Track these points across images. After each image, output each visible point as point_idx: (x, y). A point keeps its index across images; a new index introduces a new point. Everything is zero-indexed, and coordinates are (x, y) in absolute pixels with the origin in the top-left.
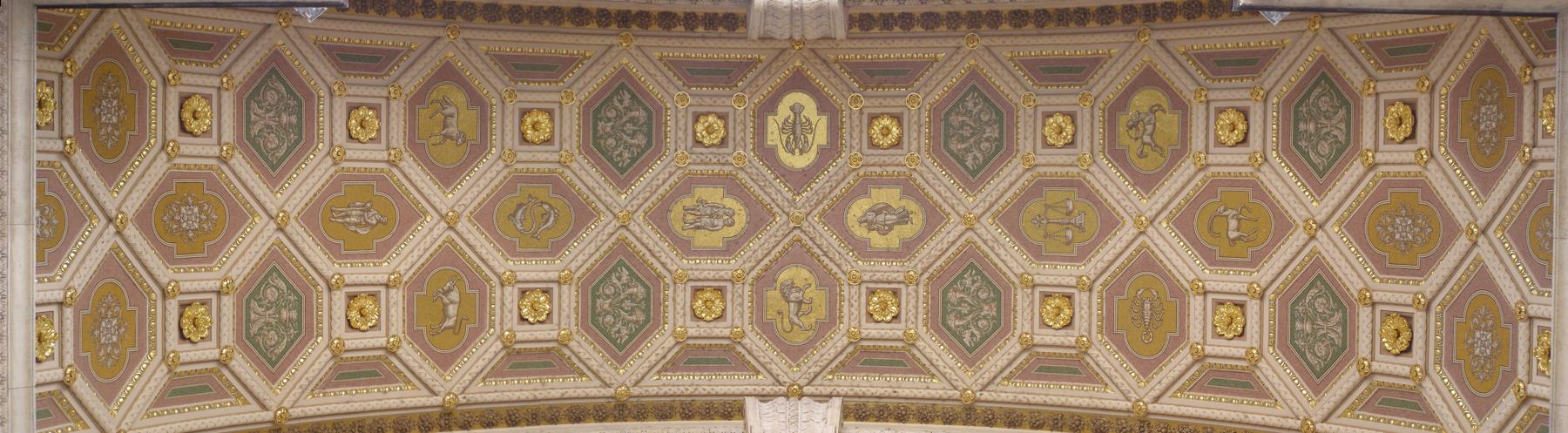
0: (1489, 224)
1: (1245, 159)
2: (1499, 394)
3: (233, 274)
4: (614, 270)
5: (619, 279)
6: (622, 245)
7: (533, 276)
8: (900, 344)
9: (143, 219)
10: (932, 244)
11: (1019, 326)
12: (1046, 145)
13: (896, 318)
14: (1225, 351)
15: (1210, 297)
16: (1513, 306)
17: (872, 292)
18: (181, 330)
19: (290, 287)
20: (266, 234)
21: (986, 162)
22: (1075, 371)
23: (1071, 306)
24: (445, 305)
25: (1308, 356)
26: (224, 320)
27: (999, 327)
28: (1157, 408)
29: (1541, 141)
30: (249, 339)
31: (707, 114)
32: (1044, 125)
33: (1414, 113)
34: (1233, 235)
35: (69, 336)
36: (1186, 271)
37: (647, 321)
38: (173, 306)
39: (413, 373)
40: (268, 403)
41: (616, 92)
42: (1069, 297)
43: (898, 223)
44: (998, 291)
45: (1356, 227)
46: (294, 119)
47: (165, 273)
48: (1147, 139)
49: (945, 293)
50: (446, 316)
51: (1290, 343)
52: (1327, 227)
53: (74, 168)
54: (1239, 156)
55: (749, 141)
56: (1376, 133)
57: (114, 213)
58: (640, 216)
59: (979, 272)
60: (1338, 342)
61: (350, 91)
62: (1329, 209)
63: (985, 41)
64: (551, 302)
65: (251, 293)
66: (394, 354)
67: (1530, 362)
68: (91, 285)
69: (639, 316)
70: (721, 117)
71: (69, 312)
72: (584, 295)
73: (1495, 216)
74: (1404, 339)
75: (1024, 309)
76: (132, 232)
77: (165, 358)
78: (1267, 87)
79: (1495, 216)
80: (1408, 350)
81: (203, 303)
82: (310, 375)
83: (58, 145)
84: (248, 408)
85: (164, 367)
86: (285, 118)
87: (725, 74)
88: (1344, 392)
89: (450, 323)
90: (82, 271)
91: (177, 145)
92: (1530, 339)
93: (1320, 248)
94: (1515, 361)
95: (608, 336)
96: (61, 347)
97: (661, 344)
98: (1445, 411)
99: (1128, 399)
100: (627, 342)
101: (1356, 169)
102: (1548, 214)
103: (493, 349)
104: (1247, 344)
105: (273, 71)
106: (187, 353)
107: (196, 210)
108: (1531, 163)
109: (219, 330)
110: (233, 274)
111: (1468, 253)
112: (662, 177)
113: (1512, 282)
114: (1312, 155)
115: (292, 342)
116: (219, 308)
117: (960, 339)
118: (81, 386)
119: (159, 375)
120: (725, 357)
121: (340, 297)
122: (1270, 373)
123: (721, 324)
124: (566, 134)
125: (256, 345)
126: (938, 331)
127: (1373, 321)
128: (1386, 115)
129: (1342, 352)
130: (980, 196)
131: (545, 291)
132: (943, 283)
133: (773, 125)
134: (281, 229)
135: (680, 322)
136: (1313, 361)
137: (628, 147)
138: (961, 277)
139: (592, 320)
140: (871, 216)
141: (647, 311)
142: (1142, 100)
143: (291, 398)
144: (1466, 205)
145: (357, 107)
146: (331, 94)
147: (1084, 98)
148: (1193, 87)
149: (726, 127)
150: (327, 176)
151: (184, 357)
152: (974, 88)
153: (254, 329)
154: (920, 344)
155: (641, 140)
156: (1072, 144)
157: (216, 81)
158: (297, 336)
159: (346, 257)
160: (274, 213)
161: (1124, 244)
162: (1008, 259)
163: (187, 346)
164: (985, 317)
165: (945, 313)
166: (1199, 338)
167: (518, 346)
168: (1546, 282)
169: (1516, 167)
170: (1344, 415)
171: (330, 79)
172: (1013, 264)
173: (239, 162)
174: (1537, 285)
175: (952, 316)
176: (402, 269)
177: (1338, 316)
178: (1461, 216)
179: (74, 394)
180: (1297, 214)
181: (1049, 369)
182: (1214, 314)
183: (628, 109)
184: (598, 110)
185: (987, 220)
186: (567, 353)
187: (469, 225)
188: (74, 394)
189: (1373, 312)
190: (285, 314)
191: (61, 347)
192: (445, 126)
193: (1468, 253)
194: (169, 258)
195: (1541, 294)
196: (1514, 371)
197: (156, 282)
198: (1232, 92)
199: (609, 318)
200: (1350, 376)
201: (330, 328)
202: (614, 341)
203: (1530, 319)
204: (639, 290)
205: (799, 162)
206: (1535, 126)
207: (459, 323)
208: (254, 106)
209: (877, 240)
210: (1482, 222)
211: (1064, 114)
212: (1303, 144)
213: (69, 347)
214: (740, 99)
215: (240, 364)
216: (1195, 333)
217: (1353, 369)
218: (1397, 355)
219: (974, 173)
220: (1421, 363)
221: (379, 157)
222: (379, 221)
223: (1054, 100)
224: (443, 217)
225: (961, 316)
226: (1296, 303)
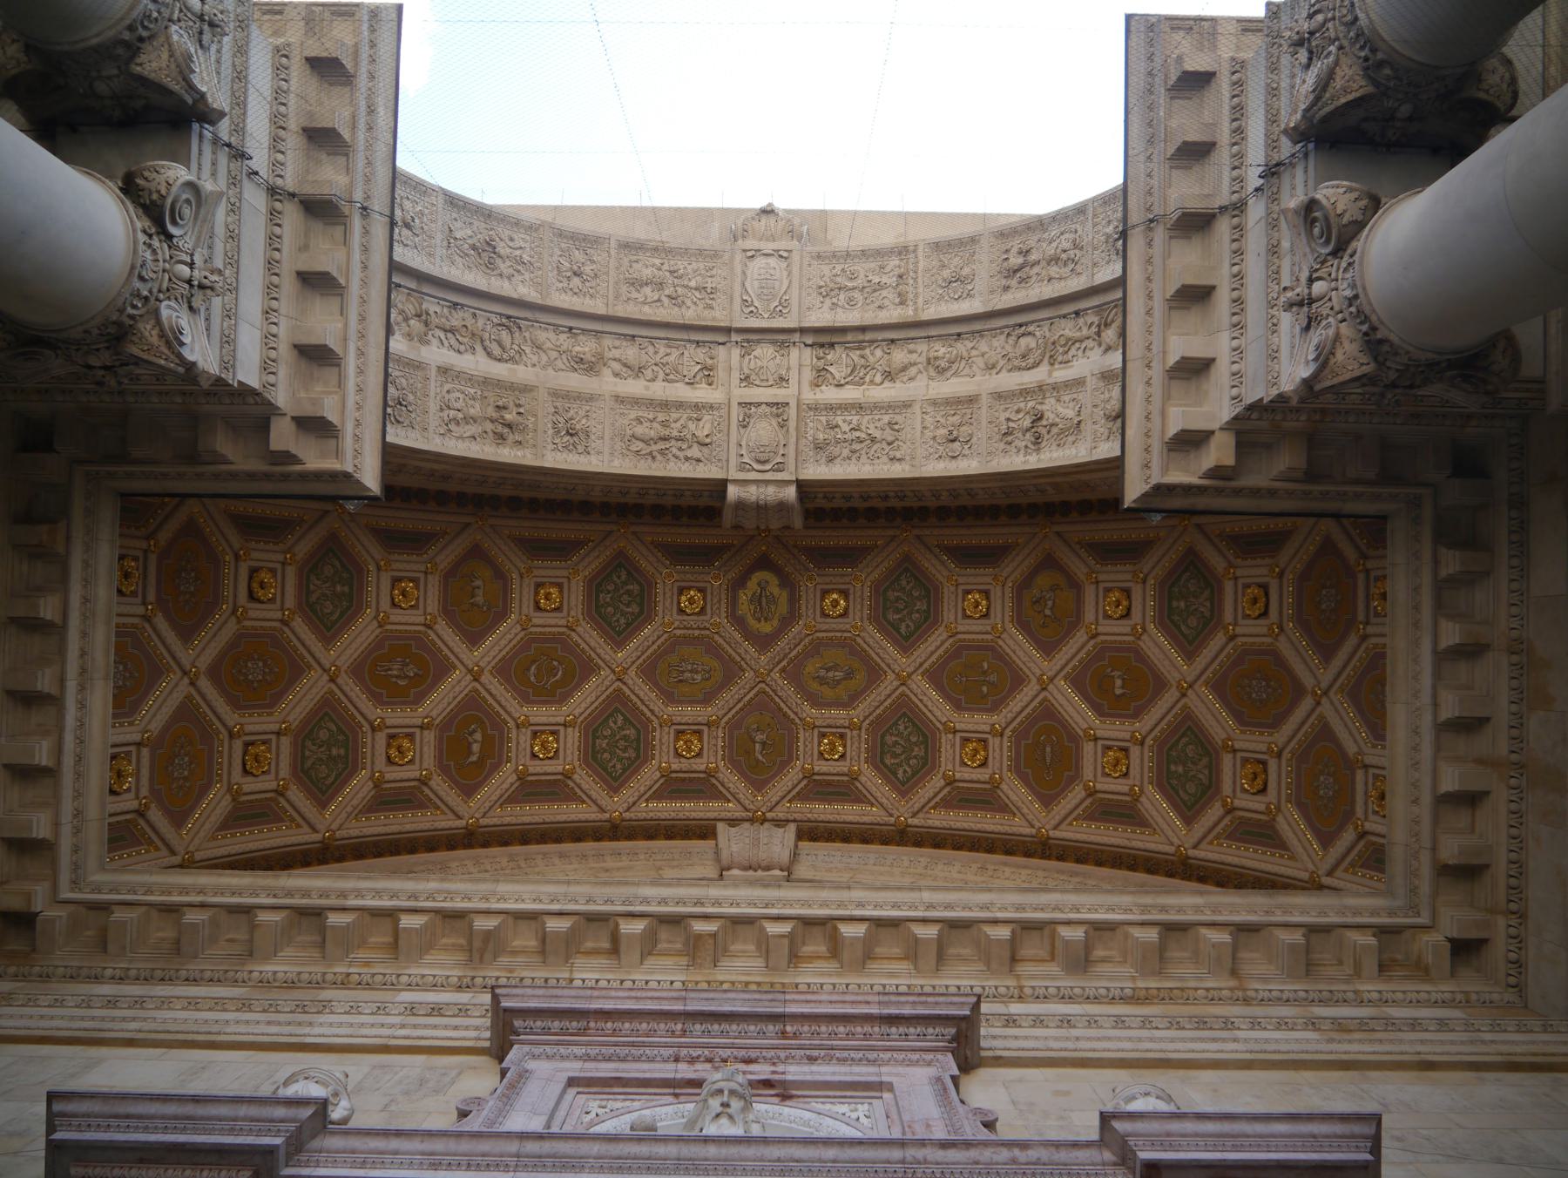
0: (1330, 686)
1: (1128, 630)
2: (1341, 828)
3: (291, 718)
4: (611, 715)
5: (615, 723)
6: (618, 696)
7: (544, 720)
8: (846, 778)
9: (214, 672)
10: (873, 696)
11: (943, 764)
12: (966, 616)
13: (843, 756)
14: (1112, 787)
15: (1100, 743)
16: (1351, 755)
17: (823, 735)
18: (244, 765)
19: (339, 729)
20: (320, 684)
21: (917, 628)
22: (988, 803)
23: (986, 748)
24: (470, 745)
25: (1181, 792)
26: (282, 757)
27: (927, 765)
28: (1057, 834)
29: (1373, 620)
30: (303, 773)
31: (690, 588)
32: (964, 600)
33: (1267, 594)
34: (1118, 692)
35: (145, 772)
36: (1080, 721)
37: (638, 757)
38: (238, 745)
39: (442, 800)
40: (319, 827)
42: (985, 741)
43: (845, 679)
44: (926, 736)
45: (1219, 687)
46: (346, 589)
47: (232, 718)
48: (1048, 612)
49: (883, 736)
50: (470, 753)
51: (1167, 783)
52: (1196, 687)
53: (155, 630)
54: (1124, 627)
55: (723, 609)
56: (1236, 610)
57: (188, 668)
58: (632, 672)
59: (910, 720)
60: (1205, 781)
61: (395, 566)
62: (1197, 672)
63: (916, 532)
64: (557, 742)
65: (305, 734)
66: (426, 784)
67: (1366, 803)
68: (166, 728)
69: (631, 753)
70: (701, 590)
71: (145, 751)
72: (586, 735)
73: (1335, 680)
74: (1259, 781)
75: (948, 750)
76: (204, 684)
77: (229, 789)
78: (1145, 571)
79: (1335, 680)
80: (1263, 791)
81: (264, 743)
82: (355, 802)
83: (140, 610)
84: (301, 830)
85: (228, 797)
86: (339, 588)
87: (703, 556)
88: (1210, 824)
89: (474, 758)
90: (158, 717)
91: (245, 611)
92: (1366, 784)
93: (1190, 704)
94: (1353, 802)
95: (605, 769)
96: (138, 781)
97: (648, 776)
98: (1295, 842)
99: (1032, 826)
100: (621, 775)
101: (1218, 640)
102: (1382, 682)
103: (510, 780)
104: (1130, 782)
106: (250, 785)
107: (261, 664)
108: (1364, 638)
109: (277, 764)
110: (291, 718)
111: (1313, 710)
112: (651, 639)
113: (1350, 734)
114: (1183, 628)
115: (340, 774)
116: (278, 747)
117: (895, 774)
118: (155, 815)
119: (224, 803)
120: (702, 786)
121: (381, 738)
122: (1148, 805)
123: (698, 760)
124: (573, 603)
126: (876, 768)
127: (1234, 765)
128: (1243, 595)
129: (1209, 790)
130: (913, 657)
131: (553, 733)
132: (880, 726)
133: (743, 597)
134: (332, 680)
135: (665, 759)
136: (1186, 798)
137: (624, 614)
138: (896, 723)
139: (591, 757)
140: (822, 673)
141: (637, 750)
142: (1044, 580)
143: (338, 822)
144: (1311, 671)
145: (400, 580)
146: (379, 568)
147: (995, 578)
148: (1085, 570)
149: (704, 599)
150: (372, 637)
151: (246, 788)
152: (907, 570)
153: (309, 763)
154: (863, 779)
155: (635, 608)
156: (986, 616)
157: (280, 557)
159: (388, 703)
160: (327, 666)
161: (1029, 698)
162: (935, 709)
163: (250, 779)
164: (915, 757)
165: (882, 753)
166: (1091, 777)
167: (530, 778)
168: (1381, 737)
169: (1352, 640)
170: (1211, 843)
171: (377, 556)
172: (938, 714)
173: (299, 624)
174: (1371, 738)
175: (888, 756)
176: (434, 714)
177: (1205, 761)
178: (1308, 681)
179: (148, 821)
180: (1172, 676)
181: (967, 801)
182: (1103, 756)
183: (625, 583)
184: (599, 585)
185: (917, 678)
186: (571, 784)
187: (491, 678)
188: (148, 821)
189: (1234, 758)
190: (334, 752)
191: (138, 781)
192: (473, 597)
193: (1313, 710)
194: (235, 704)
195: (1374, 746)
196: (1352, 812)
197: (224, 725)
198: (1117, 574)
199: (606, 755)
200: (1214, 812)
201: (373, 763)
202: (610, 774)
203: (1366, 767)
204: (631, 732)
205: (766, 628)
206: (1367, 607)
207: (482, 760)
208: (313, 577)
209: (828, 692)
210: (1324, 685)
211: (980, 591)
212: (1176, 618)
213: (145, 781)
214: (716, 577)
215: (296, 794)
216: (1088, 772)
217: (1218, 805)
218: (1254, 794)
219: (907, 638)
220: (1274, 801)
221: (417, 621)
222: (416, 674)
223: (971, 579)
224: (470, 671)
225: (895, 756)
226: (1170, 749)
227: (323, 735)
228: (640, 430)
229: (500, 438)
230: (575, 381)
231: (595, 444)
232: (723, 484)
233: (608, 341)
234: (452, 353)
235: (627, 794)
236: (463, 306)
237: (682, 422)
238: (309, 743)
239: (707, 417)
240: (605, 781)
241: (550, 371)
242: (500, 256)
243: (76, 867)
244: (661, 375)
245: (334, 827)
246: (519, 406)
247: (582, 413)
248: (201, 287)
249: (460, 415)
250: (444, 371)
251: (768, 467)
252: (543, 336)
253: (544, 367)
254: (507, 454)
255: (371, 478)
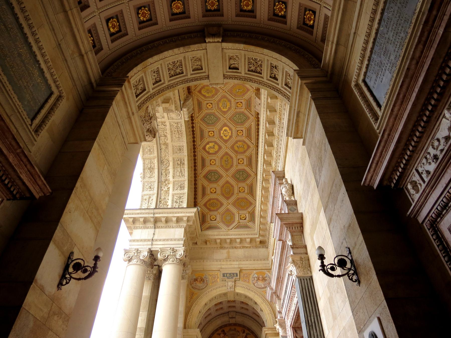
41: (205, 121)
50: (242, 147)
86: (213, 175)
89: (243, 146)
105: (206, 177)
123: (243, 103)
125: (246, 178)
131: (238, 131)
133: (207, 95)
137: (213, 118)
145: (210, 163)
153: (243, 179)
158: (244, 172)
183: (207, 118)
184: (208, 123)
190: (241, 174)
202: (246, 119)
227: (238, 176)
228: (177, 136)
229: (183, 164)
230: (170, 148)
231: (181, 145)
232: (185, 121)
233: (161, 142)
234: (170, 174)
235: (250, 116)
236: (161, 172)
237: (174, 128)
238: (240, 179)
239: (172, 124)
240: (247, 120)
241: (169, 153)
242: (151, 166)
243: (254, 234)
244: (166, 131)
245: (254, 174)
246: (177, 160)
247: (176, 148)
248: (173, 251)
249: (181, 173)
250: (173, 177)
251: (180, 114)
252: (163, 156)
253: (169, 154)
254: (186, 162)
255: (195, 210)
